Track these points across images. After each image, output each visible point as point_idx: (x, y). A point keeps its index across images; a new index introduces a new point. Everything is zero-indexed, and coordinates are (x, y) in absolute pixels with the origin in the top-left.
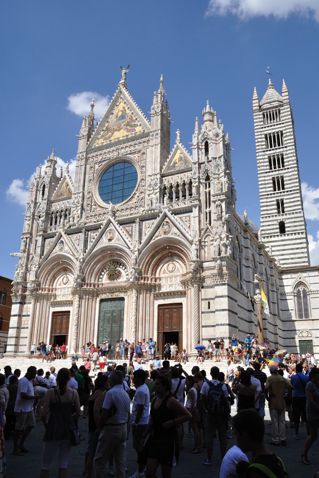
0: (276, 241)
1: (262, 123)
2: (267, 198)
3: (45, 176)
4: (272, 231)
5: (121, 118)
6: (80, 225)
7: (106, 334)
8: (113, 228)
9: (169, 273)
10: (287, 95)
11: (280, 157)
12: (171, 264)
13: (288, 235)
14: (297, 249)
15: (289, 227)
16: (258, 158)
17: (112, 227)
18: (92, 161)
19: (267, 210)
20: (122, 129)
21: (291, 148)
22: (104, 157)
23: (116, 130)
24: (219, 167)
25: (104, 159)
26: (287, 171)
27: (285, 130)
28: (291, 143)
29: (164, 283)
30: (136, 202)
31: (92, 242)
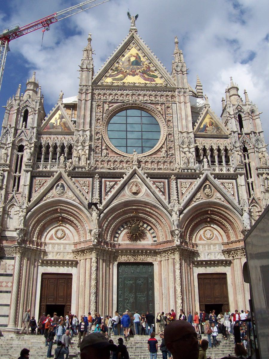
3: (29, 100)
5: (135, 63)
6: (91, 168)
7: (128, 306)
8: (140, 180)
9: (206, 240)
12: (208, 230)
17: (137, 179)
18: (100, 99)
20: (137, 75)
22: (116, 98)
23: (130, 74)
24: (259, 142)
25: (116, 101)
29: (201, 250)
30: (164, 157)
31: (109, 191)
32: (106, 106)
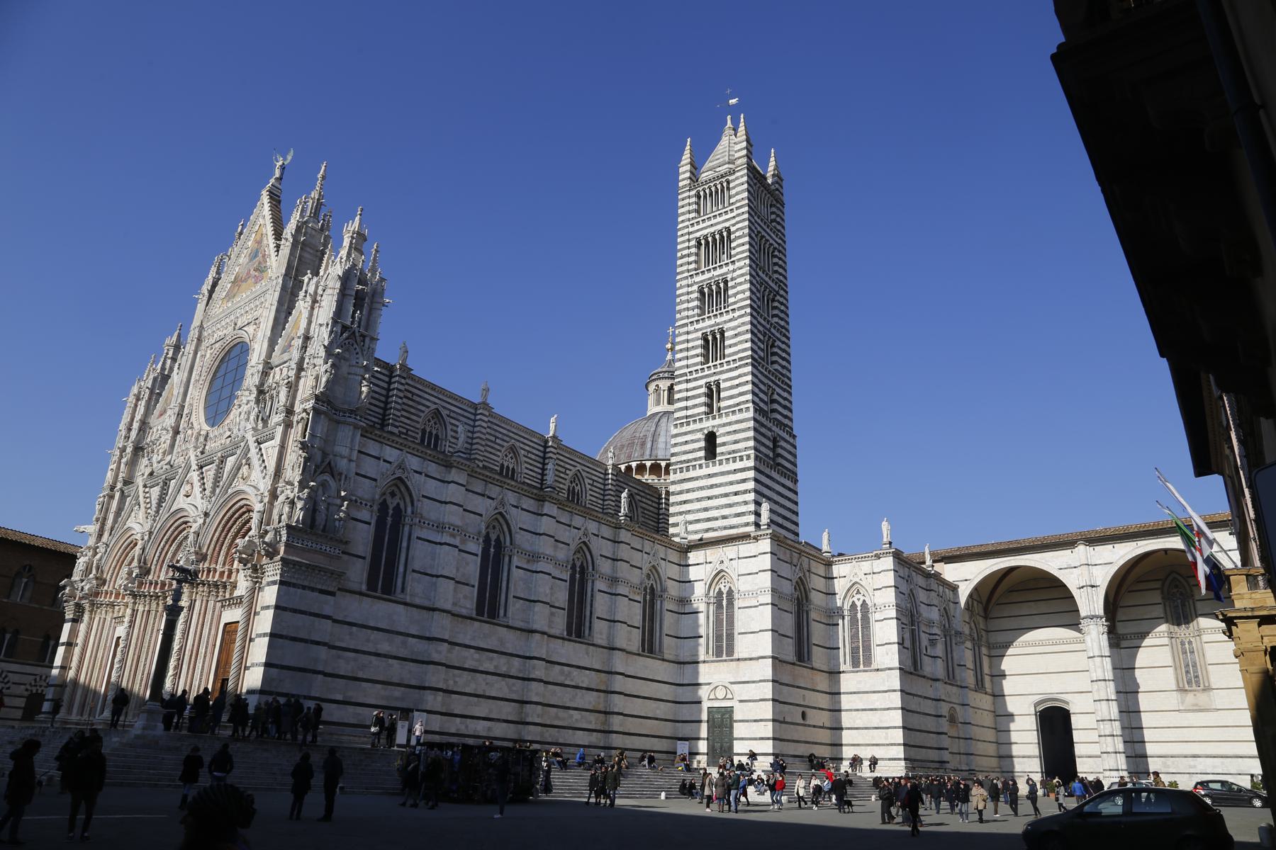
0: (696, 479)
1: (693, 215)
2: (687, 381)
4: (690, 456)
10: (744, 149)
11: (722, 285)
13: (721, 461)
14: (736, 494)
15: (724, 444)
16: (678, 292)
19: (687, 408)
21: (742, 263)
22: (220, 333)
26: (731, 316)
27: (733, 225)
28: (743, 252)
32: (209, 352)
